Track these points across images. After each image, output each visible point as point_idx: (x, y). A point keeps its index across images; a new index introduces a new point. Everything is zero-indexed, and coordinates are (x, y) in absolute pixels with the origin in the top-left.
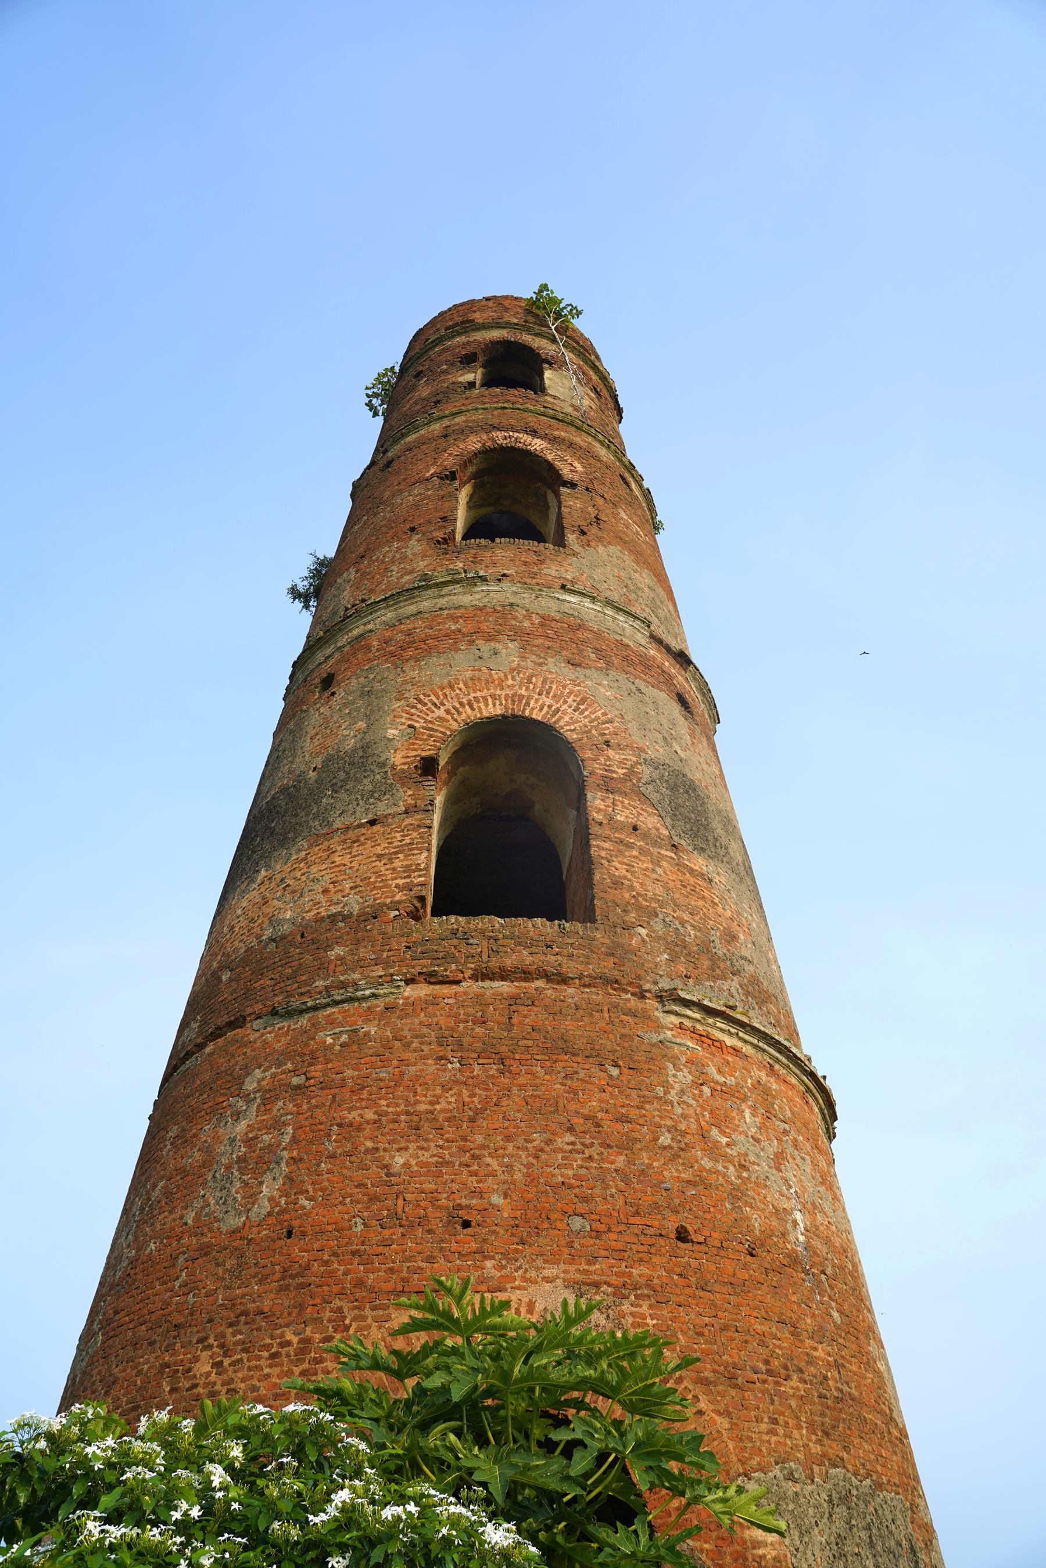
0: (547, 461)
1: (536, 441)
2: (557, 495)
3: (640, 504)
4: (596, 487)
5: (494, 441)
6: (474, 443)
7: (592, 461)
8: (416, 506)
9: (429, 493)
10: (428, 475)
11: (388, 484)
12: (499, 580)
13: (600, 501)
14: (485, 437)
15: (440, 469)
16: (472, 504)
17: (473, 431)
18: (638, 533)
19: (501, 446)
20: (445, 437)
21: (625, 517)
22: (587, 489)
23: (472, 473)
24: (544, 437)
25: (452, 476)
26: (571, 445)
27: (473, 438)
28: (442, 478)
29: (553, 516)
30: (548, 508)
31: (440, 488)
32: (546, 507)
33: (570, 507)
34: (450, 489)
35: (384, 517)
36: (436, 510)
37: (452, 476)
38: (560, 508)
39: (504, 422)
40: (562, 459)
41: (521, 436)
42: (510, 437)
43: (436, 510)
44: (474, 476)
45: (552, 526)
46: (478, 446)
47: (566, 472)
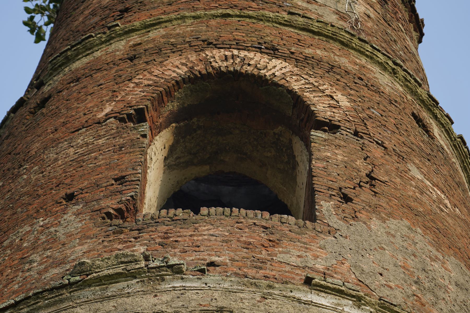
0: (291, 92)
1: (275, 62)
2: (307, 142)
3: (446, 159)
4: (371, 131)
5: (207, 62)
6: (176, 67)
7: (365, 92)
8: (79, 162)
9: (100, 142)
10: (101, 115)
11: (39, 131)
12: (202, 271)
13: (377, 152)
14: (193, 57)
15: (121, 105)
16: (172, 162)
17: (176, 49)
18: (440, 201)
19: (220, 74)
20: (131, 59)
21: (420, 176)
22: (356, 133)
23: (172, 112)
24: (289, 57)
25: (139, 116)
26: (332, 68)
27: (175, 60)
28: (122, 120)
29: (302, 179)
30: (295, 165)
31: (119, 134)
32: (293, 164)
33: (326, 159)
34: (134, 135)
35: (28, 182)
36: (109, 167)
37: (139, 116)
38: (310, 161)
39: (226, 36)
40: (316, 89)
41: (251, 55)
42: (233, 57)
43: (109, 167)
44: (175, 117)
45: (302, 193)
46: (183, 71)
47: (321, 108)
